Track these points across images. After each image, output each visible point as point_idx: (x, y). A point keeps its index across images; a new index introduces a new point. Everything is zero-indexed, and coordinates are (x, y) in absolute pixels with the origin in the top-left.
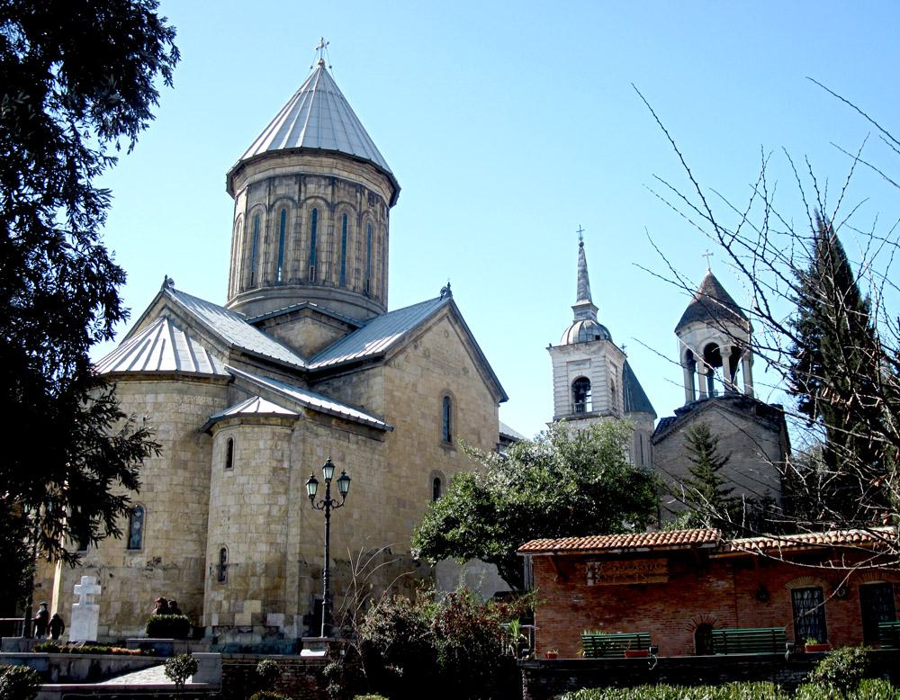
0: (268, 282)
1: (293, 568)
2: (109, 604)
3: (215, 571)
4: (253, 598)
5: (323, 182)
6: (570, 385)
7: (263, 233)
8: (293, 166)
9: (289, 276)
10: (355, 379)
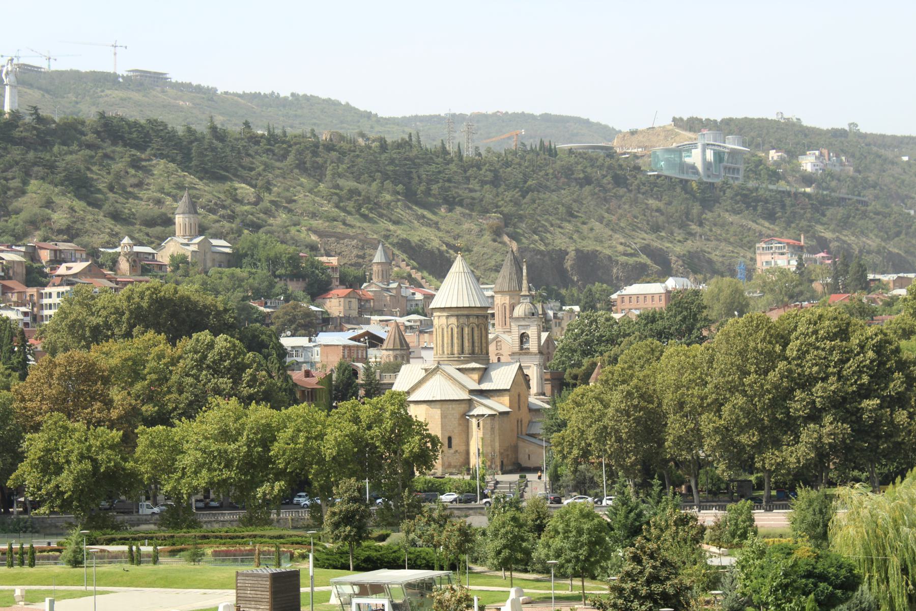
1: (497, 453)
7: (455, 335)
8: (465, 312)
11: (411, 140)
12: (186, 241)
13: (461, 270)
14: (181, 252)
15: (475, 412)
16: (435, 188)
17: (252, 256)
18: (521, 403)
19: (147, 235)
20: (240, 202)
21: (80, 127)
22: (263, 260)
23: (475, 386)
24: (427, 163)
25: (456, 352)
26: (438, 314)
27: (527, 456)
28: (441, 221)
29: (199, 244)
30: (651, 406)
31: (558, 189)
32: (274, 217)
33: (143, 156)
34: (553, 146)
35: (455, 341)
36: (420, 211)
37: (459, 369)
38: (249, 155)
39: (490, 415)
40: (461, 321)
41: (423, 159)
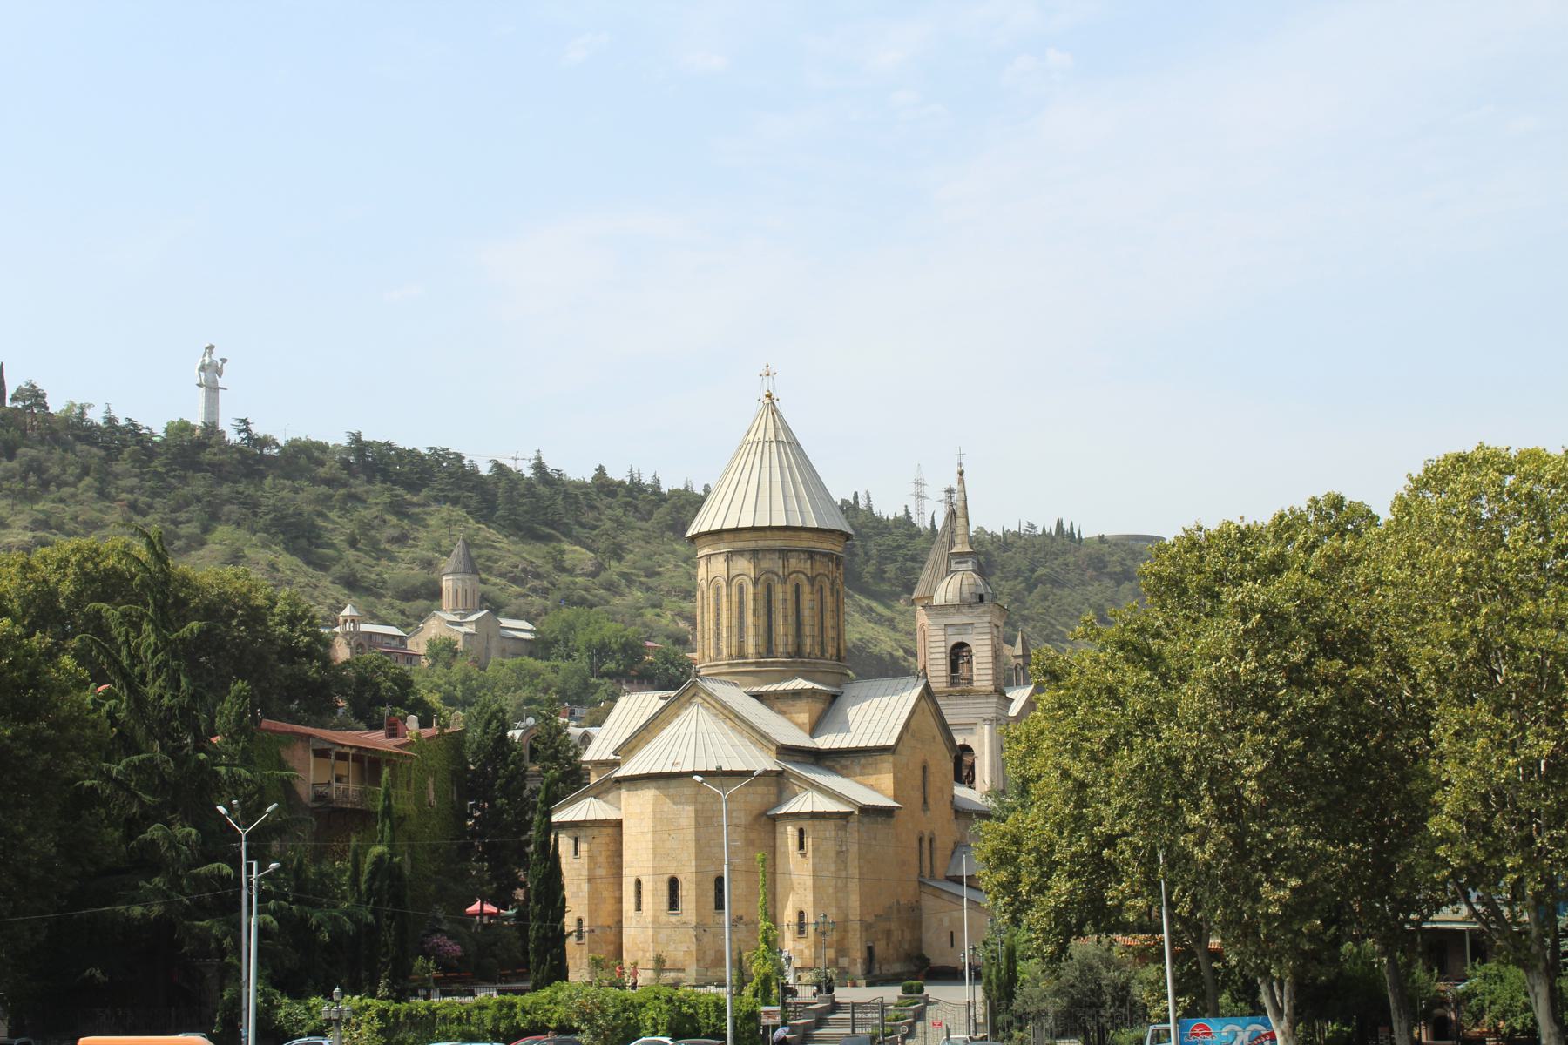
0: (759, 653)
1: (857, 926)
2: (705, 952)
3: (796, 928)
4: (829, 947)
5: (803, 556)
6: (949, 648)
8: (778, 542)
9: (781, 649)
10: (863, 761)
11: (856, 502)
12: (457, 619)
13: (771, 435)
14: (446, 634)
15: (792, 807)
16: (891, 570)
17: (566, 644)
18: (932, 790)
19: (403, 612)
20: (570, 572)
21: (316, 454)
22: (583, 648)
23: (802, 740)
24: (881, 534)
25: (751, 650)
26: (707, 551)
27: (945, 939)
28: (898, 618)
29: (477, 622)
30: (1360, 672)
31: (1083, 583)
32: (622, 595)
33: (415, 499)
34: (1076, 532)
35: (750, 620)
36: (865, 602)
37: (758, 696)
38: (592, 507)
39: (766, 773)
40: (767, 563)
41: (873, 528)
